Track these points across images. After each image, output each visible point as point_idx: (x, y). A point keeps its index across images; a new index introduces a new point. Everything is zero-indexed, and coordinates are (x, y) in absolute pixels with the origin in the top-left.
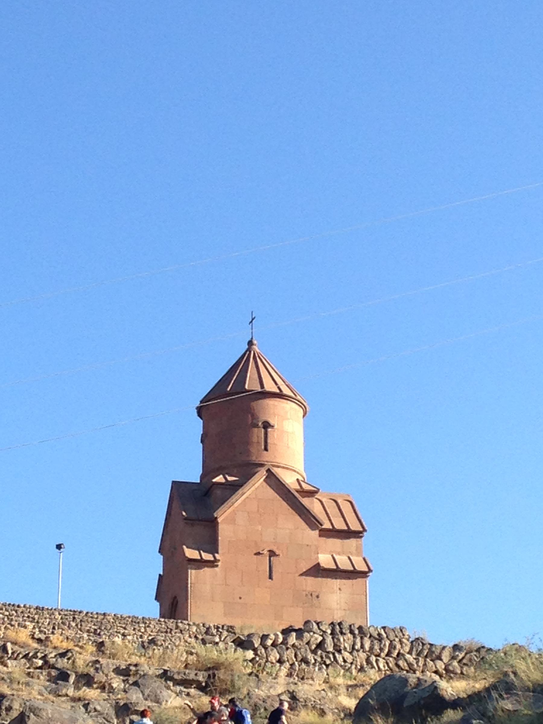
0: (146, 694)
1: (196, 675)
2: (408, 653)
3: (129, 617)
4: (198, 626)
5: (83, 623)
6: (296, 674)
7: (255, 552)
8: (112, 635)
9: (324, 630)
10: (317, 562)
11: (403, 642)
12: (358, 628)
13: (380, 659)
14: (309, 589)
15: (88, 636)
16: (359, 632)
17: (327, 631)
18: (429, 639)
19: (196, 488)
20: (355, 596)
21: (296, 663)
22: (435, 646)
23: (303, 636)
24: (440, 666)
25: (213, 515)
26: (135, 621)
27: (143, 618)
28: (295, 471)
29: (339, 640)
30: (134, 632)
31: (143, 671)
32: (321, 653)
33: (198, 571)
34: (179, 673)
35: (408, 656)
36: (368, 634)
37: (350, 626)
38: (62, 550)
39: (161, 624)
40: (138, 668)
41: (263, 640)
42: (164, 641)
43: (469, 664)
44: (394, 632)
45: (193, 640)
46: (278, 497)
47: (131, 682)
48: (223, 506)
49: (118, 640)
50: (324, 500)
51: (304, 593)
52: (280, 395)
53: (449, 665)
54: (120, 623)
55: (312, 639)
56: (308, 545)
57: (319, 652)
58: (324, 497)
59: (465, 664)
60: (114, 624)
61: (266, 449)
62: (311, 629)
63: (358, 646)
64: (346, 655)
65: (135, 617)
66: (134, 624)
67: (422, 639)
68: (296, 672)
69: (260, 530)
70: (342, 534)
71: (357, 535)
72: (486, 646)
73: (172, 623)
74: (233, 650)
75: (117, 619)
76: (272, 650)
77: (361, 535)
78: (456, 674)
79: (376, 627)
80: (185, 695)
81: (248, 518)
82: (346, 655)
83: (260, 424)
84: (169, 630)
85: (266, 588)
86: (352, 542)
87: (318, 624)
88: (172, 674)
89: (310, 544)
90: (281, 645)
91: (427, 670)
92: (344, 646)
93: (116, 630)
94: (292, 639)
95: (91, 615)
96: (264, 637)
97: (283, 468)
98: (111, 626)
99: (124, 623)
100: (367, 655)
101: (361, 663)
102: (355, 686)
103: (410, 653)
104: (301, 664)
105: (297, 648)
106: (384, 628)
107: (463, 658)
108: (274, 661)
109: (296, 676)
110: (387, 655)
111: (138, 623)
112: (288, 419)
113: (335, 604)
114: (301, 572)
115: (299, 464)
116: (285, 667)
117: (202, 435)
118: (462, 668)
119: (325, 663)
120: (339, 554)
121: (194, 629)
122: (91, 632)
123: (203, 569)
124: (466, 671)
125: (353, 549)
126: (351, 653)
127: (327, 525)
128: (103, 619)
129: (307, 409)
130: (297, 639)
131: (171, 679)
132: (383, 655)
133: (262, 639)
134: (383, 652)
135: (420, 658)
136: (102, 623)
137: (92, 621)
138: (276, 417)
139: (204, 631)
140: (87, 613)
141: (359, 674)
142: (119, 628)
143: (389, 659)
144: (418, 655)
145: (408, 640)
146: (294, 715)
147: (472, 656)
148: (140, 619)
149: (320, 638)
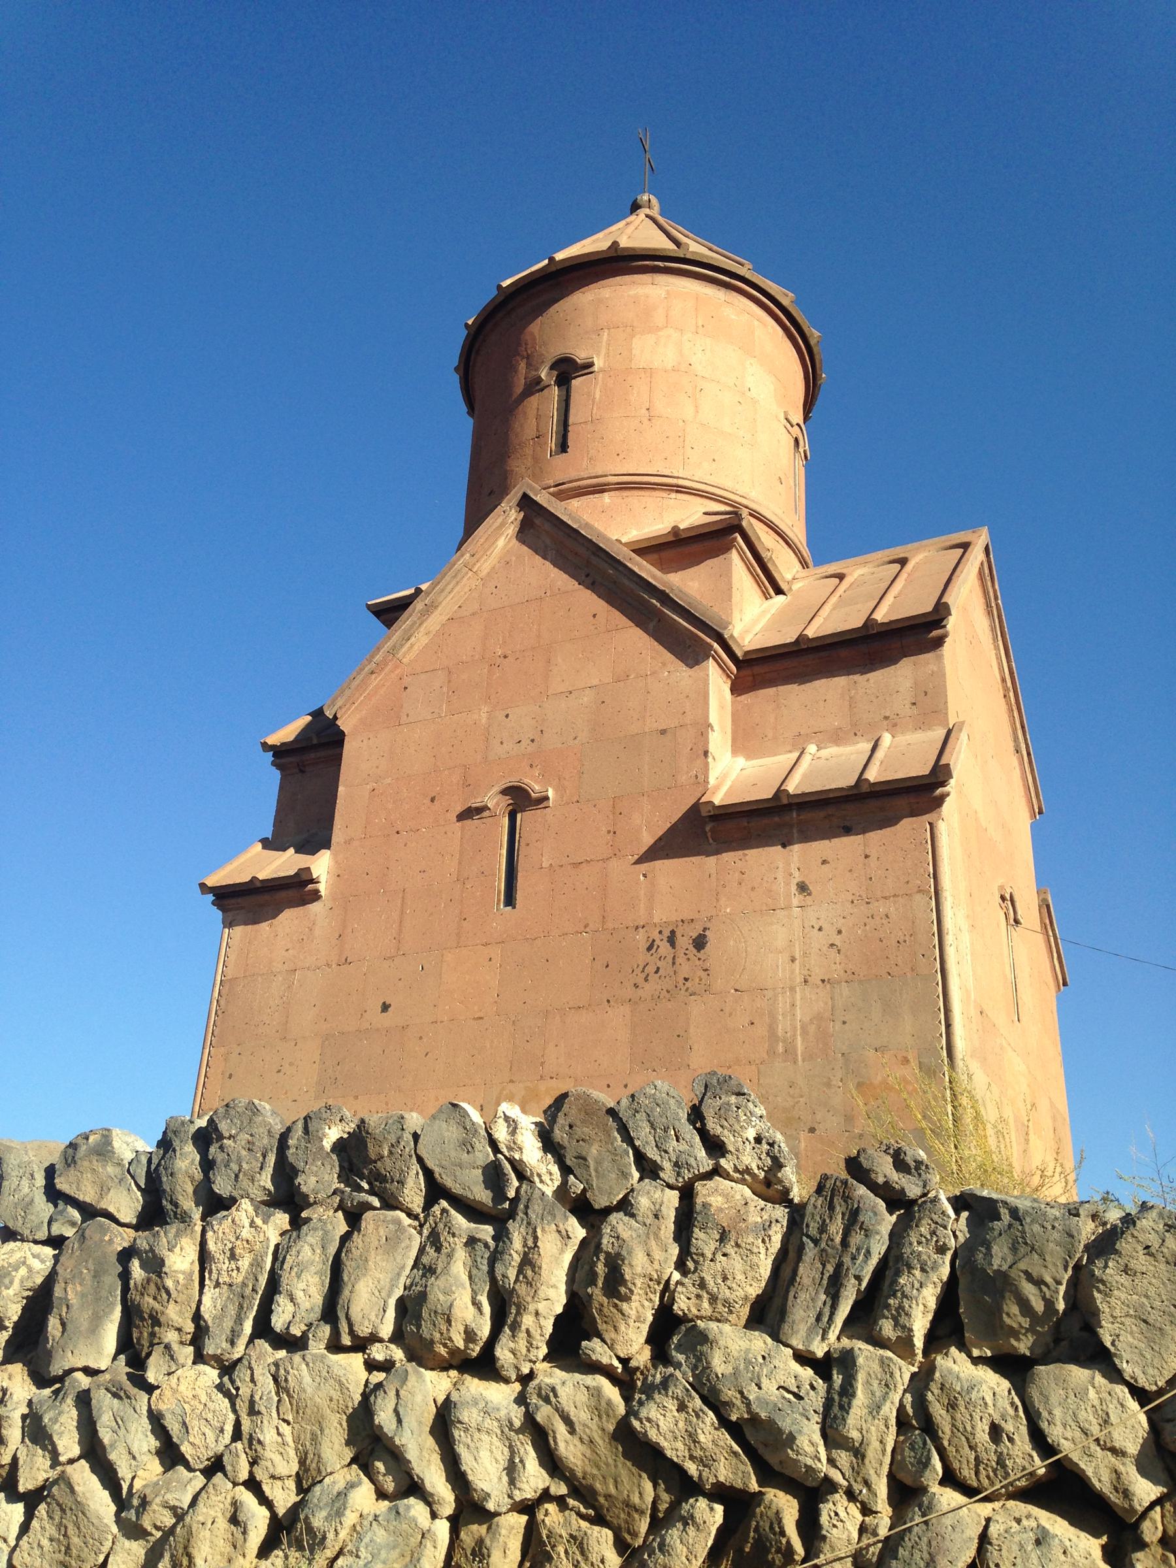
7: (459, 809)
9: (87, 1195)
14: (663, 914)
17: (103, 1205)
20: (881, 908)
22: (1014, 1212)
28: (679, 489)
29: (155, 1265)
33: (256, 926)
44: (629, 1140)
51: (641, 938)
61: (563, 447)
69: (484, 721)
70: (844, 653)
81: (445, 689)
83: (543, 376)
85: (486, 944)
101: (302, 1462)
113: (783, 959)
125: (901, 705)
129: (785, 302)
134: (515, 1327)
138: (606, 334)
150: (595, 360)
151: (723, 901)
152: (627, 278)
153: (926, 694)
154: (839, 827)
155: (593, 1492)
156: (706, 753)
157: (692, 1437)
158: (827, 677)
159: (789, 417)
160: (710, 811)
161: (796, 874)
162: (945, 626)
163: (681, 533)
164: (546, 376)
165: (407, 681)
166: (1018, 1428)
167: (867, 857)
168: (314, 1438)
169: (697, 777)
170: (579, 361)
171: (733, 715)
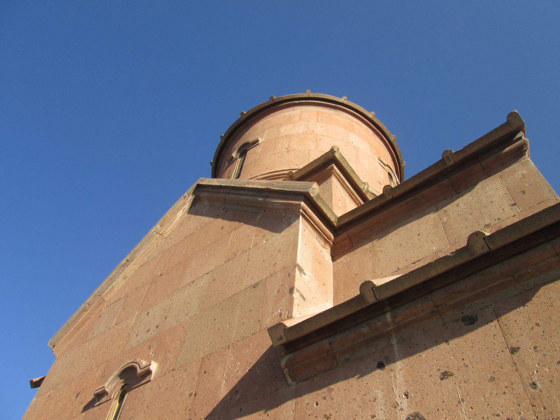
83: (234, 155)
150: (259, 139)
152: (280, 111)
153: (524, 192)
154: (456, 321)
156: (291, 291)
158: (418, 218)
159: (381, 159)
160: (281, 338)
161: (404, 403)
162: (520, 138)
163: (294, 175)
164: (236, 155)
167: (513, 351)
169: (281, 314)
170: (250, 141)
171: (334, 274)
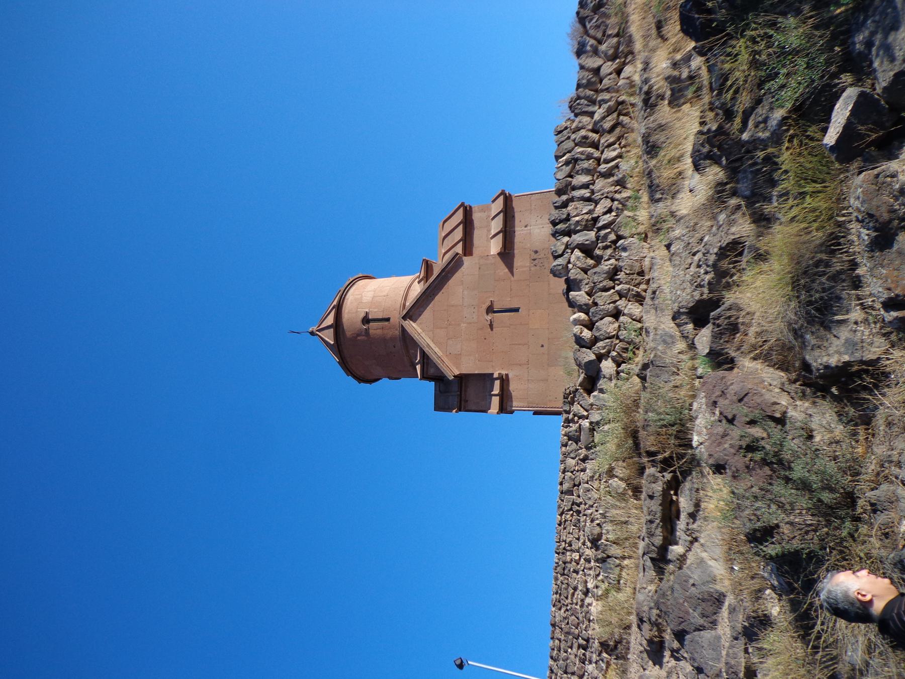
0: (701, 621)
1: (651, 497)
2: (593, 118)
3: (556, 579)
4: (566, 455)
5: (569, 670)
6: (635, 289)
7: (490, 330)
8: (588, 615)
9: (563, 247)
10: (498, 256)
11: (577, 127)
12: (559, 196)
13: (604, 156)
15: (590, 662)
16: (564, 194)
18: (572, 92)
19: (438, 389)
21: (617, 288)
22: (579, 80)
23: (576, 279)
24: (608, 68)
25: (453, 380)
26: (563, 570)
27: (556, 553)
28: (410, 287)
30: (581, 573)
31: (651, 608)
32: (599, 248)
33: (513, 397)
34: (651, 535)
35: (597, 117)
36: (567, 180)
37: (556, 208)
38: (464, 661)
39: (565, 521)
40: (645, 617)
41: (584, 344)
42: (592, 521)
43: (602, 28)
44: (563, 142)
45: (589, 465)
46: (430, 305)
47: (676, 645)
48: (442, 370)
49: (596, 608)
50: (443, 251)
51: (532, 269)
52: (339, 308)
53: (606, 55)
54: (567, 598)
55: (579, 265)
56: (479, 268)
57: (598, 252)
58: (441, 251)
59: (604, 35)
60: (568, 608)
61: (388, 320)
62: (563, 268)
63: (585, 193)
64: (600, 209)
65: (556, 567)
66: (566, 572)
67: (570, 102)
68: (632, 287)
70: (468, 229)
71: (468, 213)
72: (576, 10)
73: (563, 501)
74: (601, 395)
75: (559, 602)
76: (598, 329)
77: (468, 209)
78: (619, 43)
79: (556, 170)
80: (693, 523)
82: (600, 209)
84: (575, 508)
86: (477, 217)
87: (556, 257)
88: (653, 548)
89: (478, 266)
90: (590, 314)
91: (616, 85)
92: (587, 213)
93: (578, 607)
94: (580, 296)
95: (555, 652)
96: (580, 342)
97: (405, 299)
98: (572, 614)
99: (566, 589)
100: (597, 178)
101: (612, 185)
102: (652, 188)
103: (591, 114)
104: (618, 280)
105: (593, 288)
106: (557, 158)
107: (595, 38)
108: (616, 325)
109: (638, 288)
110: (597, 149)
111: (565, 563)
112: (362, 297)
113: (543, 230)
114: (509, 273)
115: (407, 279)
116: (625, 307)
117: (391, 378)
118: (609, 36)
119: (614, 242)
120: (489, 231)
121: (571, 462)
122: (584, 654)
123: (512, 392)
124: (614, 28)
125: (483, 215)
126: (597, 203)
127: (459, 249)
128: (561, 628)
130: (580, 290)
131: (663, 550)
132: (597, 154)
133: (582, 347)
134: (592, 154)
135: (599, 98)
136: (568, 633)
137: (566, 652)
139: (574, 444)
140: (552, 658)
141: (629, 186)
142: (575, 601)
143: (603, 144)
144: (593, 102)
145: (573, 121)
146: (749, 325)
147: (591, 27)
148: (559, 559)
149: (577, 252)
151: (526, 247)
155: (618, 137)
157: (610, 120)
165: (448, 353)
166: (609, 77)
168: (609, 183)
